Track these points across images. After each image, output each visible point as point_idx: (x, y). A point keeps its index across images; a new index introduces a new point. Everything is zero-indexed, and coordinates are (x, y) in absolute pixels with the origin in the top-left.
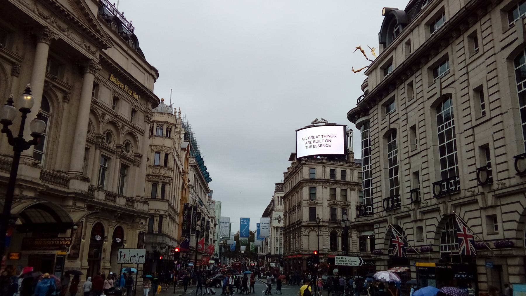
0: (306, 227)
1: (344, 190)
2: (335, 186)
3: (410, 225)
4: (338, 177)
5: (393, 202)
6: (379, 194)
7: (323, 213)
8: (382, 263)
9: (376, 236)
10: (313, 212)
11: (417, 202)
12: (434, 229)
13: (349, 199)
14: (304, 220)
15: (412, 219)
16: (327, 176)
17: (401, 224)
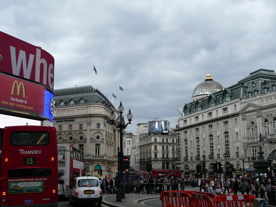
0: (153, 161)
1: (167, 146)
2: (164, 145)
3: (190, 165)
4: (165, 141)
5: (186, 159)
6: (182, 156)
7: (160, 156)
8: (183, 174)
9: (182, 167)
10: (156, 155)
11: (192, 160)
12: (195, 166)
13: (169, 149)
14: (153, 158)
15: (191, 163)
16: (161, 141)
17: (188, 164)
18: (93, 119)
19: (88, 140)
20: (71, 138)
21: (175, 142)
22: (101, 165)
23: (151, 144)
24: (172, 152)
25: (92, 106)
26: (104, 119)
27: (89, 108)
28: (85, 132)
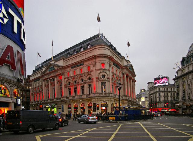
4: (166, 90)
7: (162, 99)
10: (160, 99)
11: (189, 99)
16: (163, 90)
18: (98, 60)
19: (95, 80)
20: (82, 80)
21: (173, 90)
22: (107, 102)
23: (156, 92)
24: (171, 97)
25: (96, 47)
26: (109, 59)
27: (94, 50)
28: (92, 73)
